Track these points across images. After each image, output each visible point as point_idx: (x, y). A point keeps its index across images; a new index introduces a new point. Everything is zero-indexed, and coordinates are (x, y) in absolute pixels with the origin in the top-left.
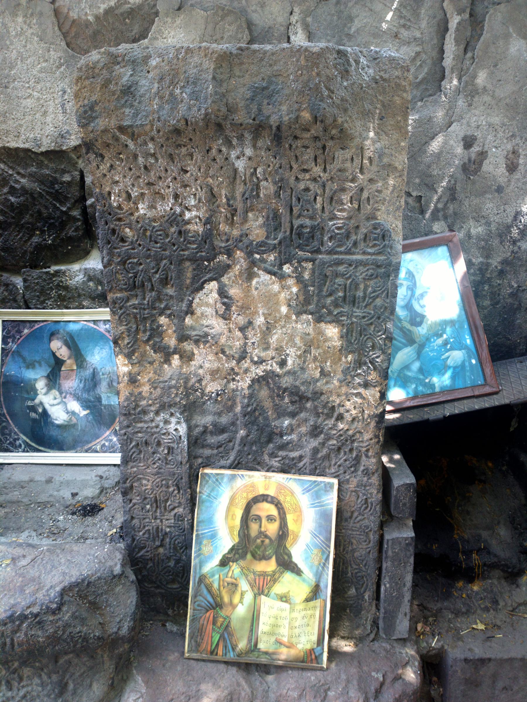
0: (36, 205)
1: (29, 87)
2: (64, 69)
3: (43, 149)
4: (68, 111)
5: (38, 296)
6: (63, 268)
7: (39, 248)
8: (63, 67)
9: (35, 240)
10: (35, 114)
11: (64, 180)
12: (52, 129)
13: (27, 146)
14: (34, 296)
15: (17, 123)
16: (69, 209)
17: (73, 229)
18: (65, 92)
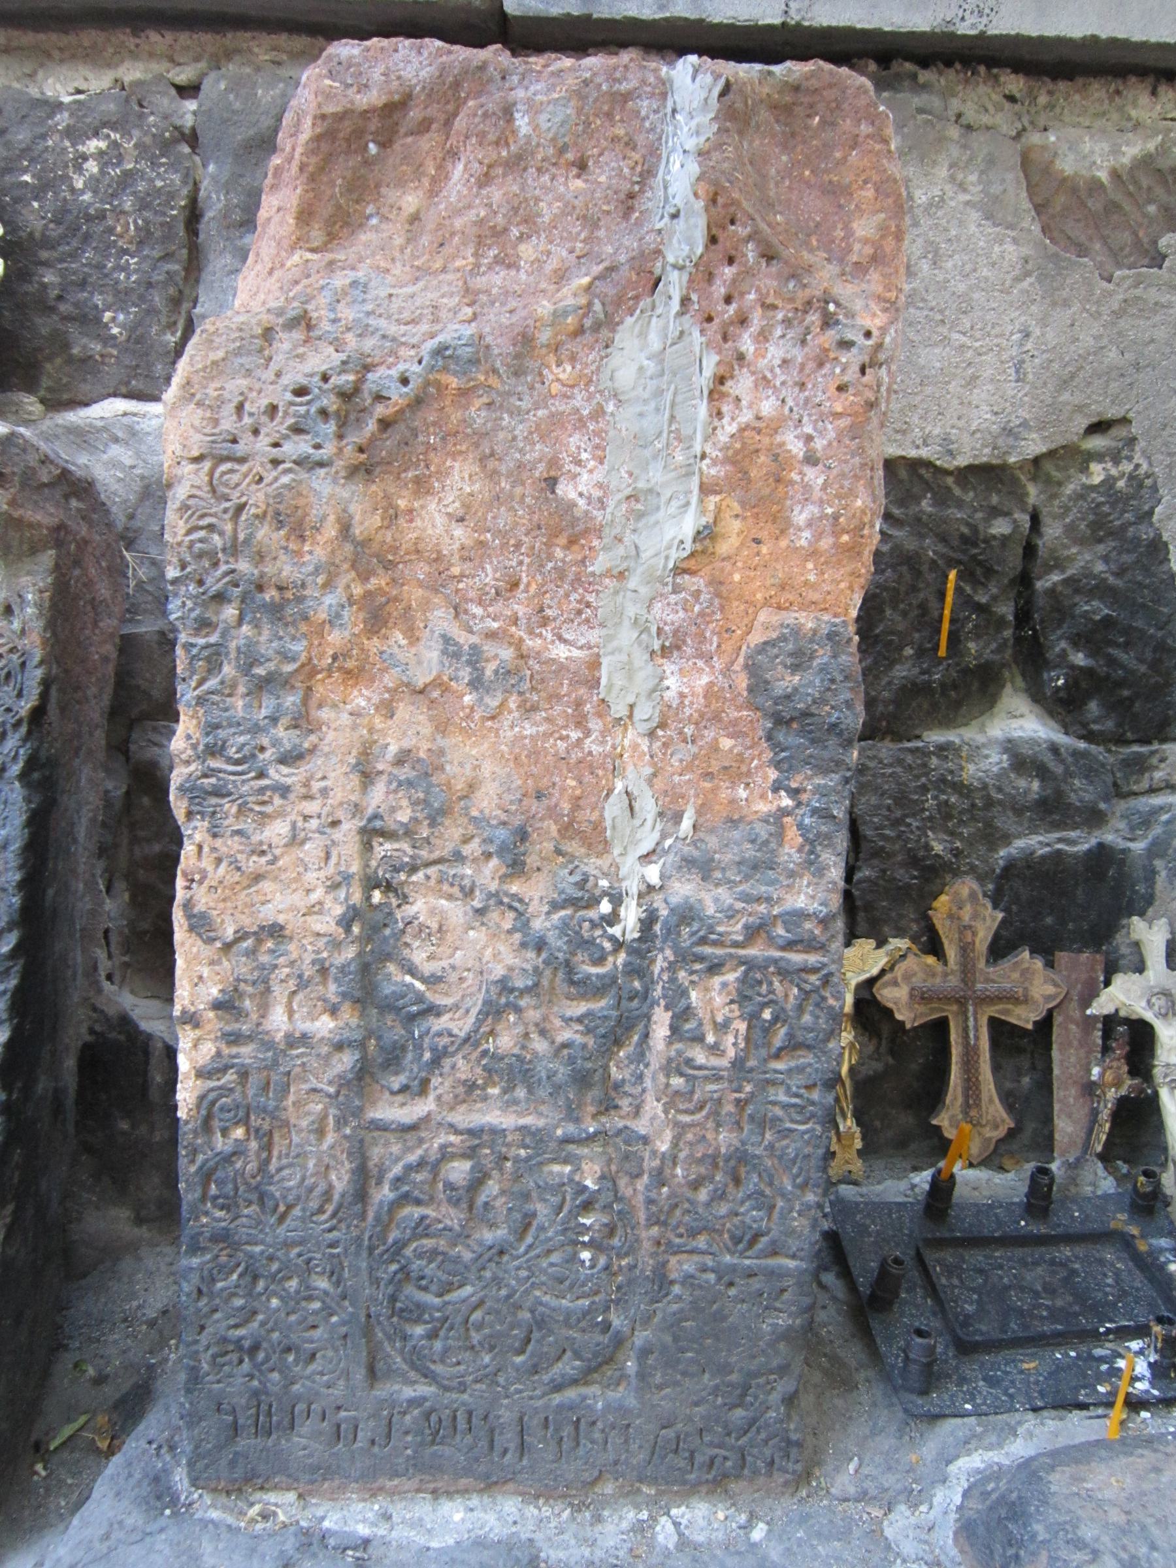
0: (919, 590)
1: (943, 321)
2: (1031, 284)
3: (962, 461)
4: (1030, 376)
5: (889, 808)
6: (951, 736)
7: (913, 691)
8: (1029, 280)
9: (901, 672)
10: (948, 383)
11: (994, 531)
12: (988, 416)
13: (924, 453)
15: (904, 402)
16: (995, 598)
17: (994, 646)
18: (1027, 335)
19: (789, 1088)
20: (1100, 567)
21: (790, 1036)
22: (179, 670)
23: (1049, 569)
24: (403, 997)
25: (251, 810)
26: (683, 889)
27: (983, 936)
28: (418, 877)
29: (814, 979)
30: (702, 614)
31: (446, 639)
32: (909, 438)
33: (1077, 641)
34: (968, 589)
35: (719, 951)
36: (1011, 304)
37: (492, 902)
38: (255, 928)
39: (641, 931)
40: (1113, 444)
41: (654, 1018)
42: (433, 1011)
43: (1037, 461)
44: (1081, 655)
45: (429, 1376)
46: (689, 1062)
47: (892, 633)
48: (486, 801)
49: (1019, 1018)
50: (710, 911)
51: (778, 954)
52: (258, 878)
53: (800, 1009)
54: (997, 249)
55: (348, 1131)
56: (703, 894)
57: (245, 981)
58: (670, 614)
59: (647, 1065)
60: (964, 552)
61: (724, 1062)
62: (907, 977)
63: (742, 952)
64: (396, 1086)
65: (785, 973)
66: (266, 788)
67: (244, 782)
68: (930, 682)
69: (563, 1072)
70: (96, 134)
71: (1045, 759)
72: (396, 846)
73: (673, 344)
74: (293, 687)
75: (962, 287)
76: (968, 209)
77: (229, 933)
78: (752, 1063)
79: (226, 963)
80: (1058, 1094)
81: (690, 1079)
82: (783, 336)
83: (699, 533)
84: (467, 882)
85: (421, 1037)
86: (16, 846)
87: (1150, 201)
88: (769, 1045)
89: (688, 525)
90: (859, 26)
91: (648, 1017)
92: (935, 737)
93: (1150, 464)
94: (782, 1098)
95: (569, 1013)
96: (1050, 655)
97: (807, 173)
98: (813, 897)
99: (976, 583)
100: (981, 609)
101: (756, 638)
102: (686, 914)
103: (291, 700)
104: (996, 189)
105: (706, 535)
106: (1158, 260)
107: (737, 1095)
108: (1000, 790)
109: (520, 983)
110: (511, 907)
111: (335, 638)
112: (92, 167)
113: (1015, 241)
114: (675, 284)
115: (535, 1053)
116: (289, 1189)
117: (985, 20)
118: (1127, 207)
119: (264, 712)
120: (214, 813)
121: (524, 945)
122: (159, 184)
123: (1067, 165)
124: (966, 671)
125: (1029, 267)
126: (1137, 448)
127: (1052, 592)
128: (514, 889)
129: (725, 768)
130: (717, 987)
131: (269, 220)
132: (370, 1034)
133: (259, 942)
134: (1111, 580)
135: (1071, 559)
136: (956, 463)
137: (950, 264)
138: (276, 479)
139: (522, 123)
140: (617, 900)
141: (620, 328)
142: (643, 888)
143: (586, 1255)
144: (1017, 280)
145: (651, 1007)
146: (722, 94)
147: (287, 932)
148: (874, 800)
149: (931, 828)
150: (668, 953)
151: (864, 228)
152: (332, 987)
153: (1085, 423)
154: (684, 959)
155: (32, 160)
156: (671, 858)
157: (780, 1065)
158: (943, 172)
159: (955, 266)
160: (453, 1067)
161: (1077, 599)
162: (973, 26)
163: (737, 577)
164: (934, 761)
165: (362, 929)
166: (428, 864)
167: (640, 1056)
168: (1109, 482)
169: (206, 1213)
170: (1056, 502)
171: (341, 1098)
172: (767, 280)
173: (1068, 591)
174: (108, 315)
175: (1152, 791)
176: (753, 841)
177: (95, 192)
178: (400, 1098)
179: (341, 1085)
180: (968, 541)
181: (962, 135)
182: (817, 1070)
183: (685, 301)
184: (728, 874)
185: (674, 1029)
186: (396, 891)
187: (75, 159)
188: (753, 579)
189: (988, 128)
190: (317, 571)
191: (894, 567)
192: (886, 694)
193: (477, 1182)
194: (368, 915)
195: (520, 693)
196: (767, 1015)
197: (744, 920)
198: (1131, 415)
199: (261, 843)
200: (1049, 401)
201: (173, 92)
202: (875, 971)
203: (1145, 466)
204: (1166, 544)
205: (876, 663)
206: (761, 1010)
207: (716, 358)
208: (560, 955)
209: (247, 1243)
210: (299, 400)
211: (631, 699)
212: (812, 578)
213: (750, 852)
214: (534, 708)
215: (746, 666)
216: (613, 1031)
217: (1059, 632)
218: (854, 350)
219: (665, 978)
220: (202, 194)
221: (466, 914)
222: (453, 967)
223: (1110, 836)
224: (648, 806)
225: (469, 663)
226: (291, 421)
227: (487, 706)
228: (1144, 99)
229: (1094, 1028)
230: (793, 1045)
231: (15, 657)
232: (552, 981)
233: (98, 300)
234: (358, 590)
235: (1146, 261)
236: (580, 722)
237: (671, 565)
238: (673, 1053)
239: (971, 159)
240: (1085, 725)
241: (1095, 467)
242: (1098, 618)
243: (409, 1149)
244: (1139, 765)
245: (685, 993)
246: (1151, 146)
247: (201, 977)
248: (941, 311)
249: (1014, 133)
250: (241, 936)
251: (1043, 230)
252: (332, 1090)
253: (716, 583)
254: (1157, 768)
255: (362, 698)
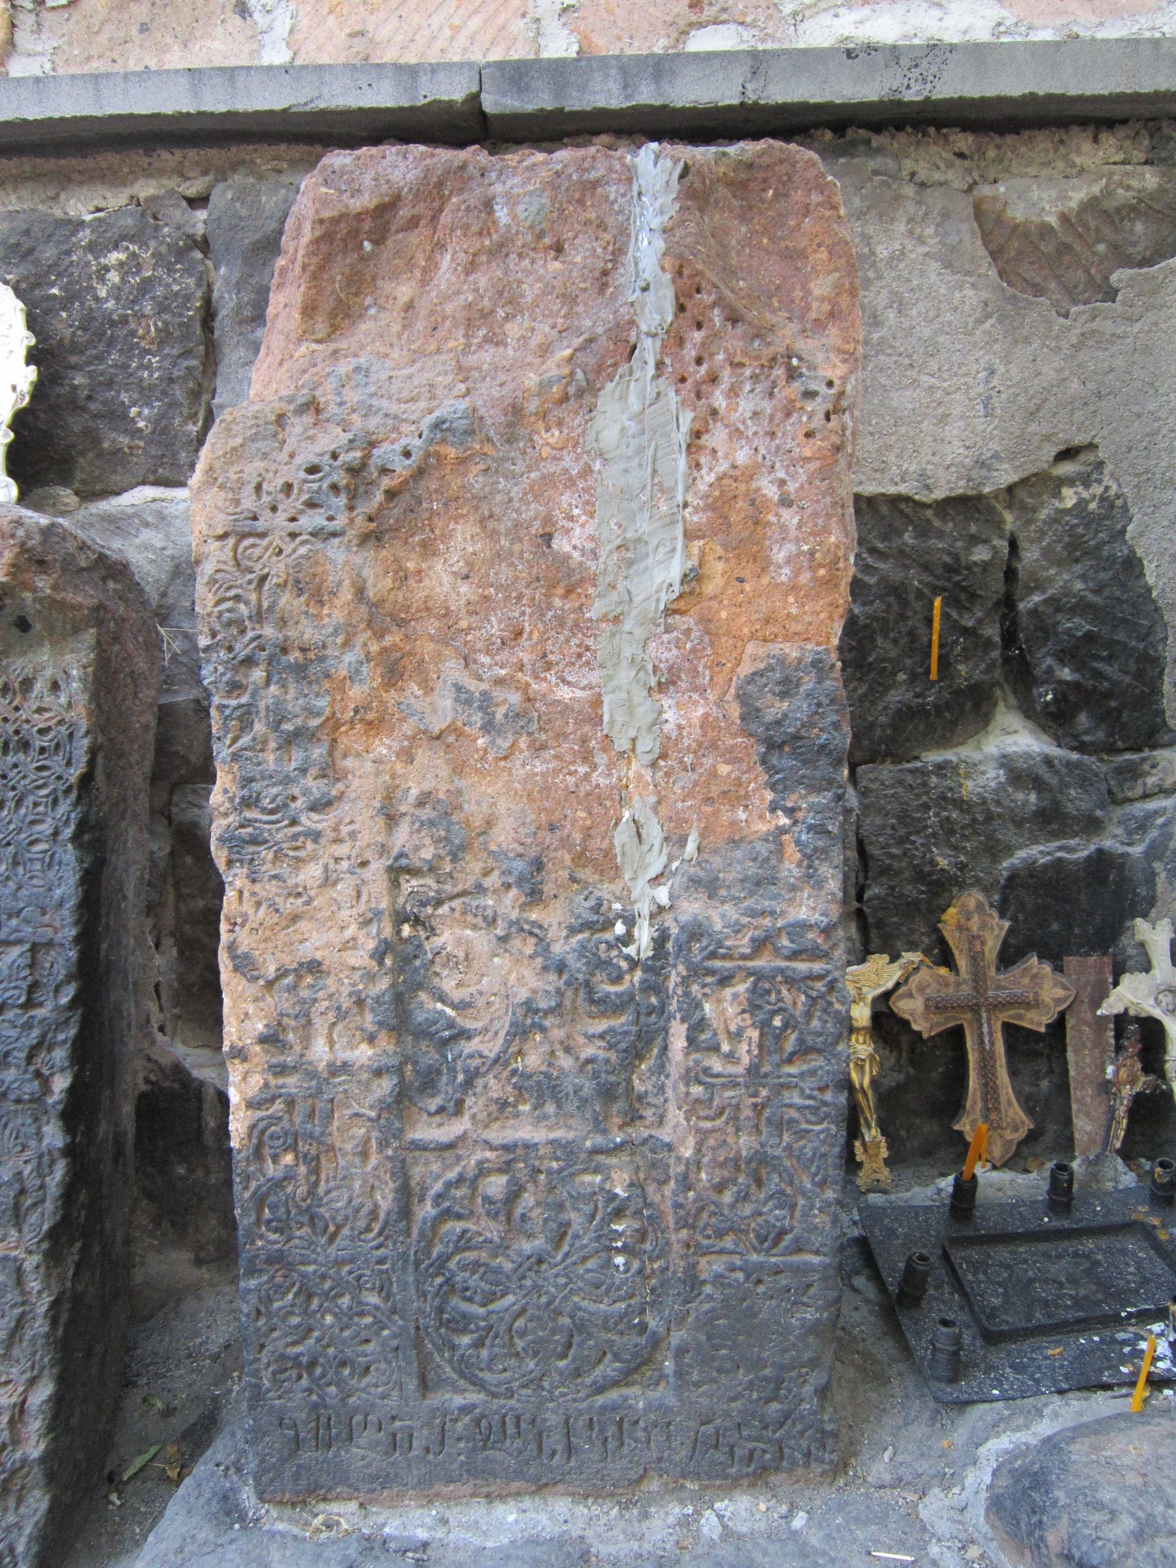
0: (907, 618)
1: (911, 365)
2: (992, 326)
3: (939, 494)
4: (998, 411)
5: (893, 828)
6: (950, 755)
7: (907, 714)
8: (990, 322)
9: (897, 697)
10: (920, 422)
13: (902, 489)
14: (883, 827)
16: (980, 621)
17: (983, 666)
18: (993, 373)
19: (802, 1090)
20: (1078, 586)
21: (801, 1041)
22: (214, 730)
23: (1030, 591)
24: (435, 1023)
25: (287, 855)
26: (692, 908)
27: (992, 946)
28: (444, 910)
29: (820, 986)
30: (693, 650)
31: (459, 688)
32: (887, 477)
33: (1062, 657)
34: (954, 615)
35: (728, 964)
36: (975, 345)
37: (513, 930)
38: (295, 965)
39: (655, 949)
40: (1083, 469)
41: (672, 1031)
42: (464, 1035)
43: (1010, 489)
44: (1067, 670)
45: (479, 1384)
46: (707, 1071)
47: (884, 660)
48: (503, 836)
49: (1031, 1021)
50: (718, 927)
51: (784, 964)
52: (295, 918)
53: (809, 1015)
54: (957, 295)
55: (390, 1152)
56: (710, 912)
57: (288, 1016)
58: (663, 653)
59: (667, 1076)
60: (949, 579)
61: (740, 1069)
62: (921, 989)
63: (750, 964)
64: (433, 1108)
65: (792, 981)
66: (299, 834)
67: (278, 830)
68: (923, 704)
69: (588, 1087)
70: (116, 247)
71: (1040, 772)
72: (422, 882)
73: (651, 405)
74: (319, 740)
75: (927, 333)
76: (928, 261)
77: (271, 971)
78: (766, 1069)
79: (269, 999)
80: (1075, 1094)
81: (709, 1087)
82: (752, 391)
83: (685, 575)
84: (489, 912)
85: (454, 1060)
86: (71, 903)
87: (1099, 241)
88: (782, 1050)
89: (675, 570)
90: (812, 101)
91: (666, 1030)
92: (933, 757)
93: (1119, 486)
94: (797, 1100)
95: (591, 1031)
96: (1038, 672)
97: (765, 241)
98: (814, 909)
99: (961, 608)
100: (965, 631)
101: (746, 669)
102: (695, 932)
103: (318, 752)
104: (953, 240)
105: (693, 578)
106: (1111, 294)
107: (754, 1100)
108: (998, 803)
109: (543, 1004)
110: (531, 933)
111: (356, 693)
112: (114, 277)
113: (974, 286)
114: (649, 350)
115: (561, 1069)
116: (337, 1210)
117: (929, 86)
118: (1078, 247)
119: (293, 765)
120: (252, 860)
121: (545, 969)
122: (176, 288)
123: (1018, 213)
124: (958, 693)
125: (989, 309)
126: (1106, 471)
127: (1034, 612)
128: (534, 916)
129: (724, 792)
130: (729, 998)
131: (277, 315)
132: (406, 1059)
133: (299, 977)
134: (1091, 597)
135: (1050, 580)
136: (933, 496)
137: (914, 312)
138: (294, 551)
139: (502, 214)
140: (630, 922)
141: (602, 393)
142: (654, 908)
143: (620, 1260)
144: (980, 322)
145: (668, 1020)
146: (682, 176)
147: (324, 968)
148: (879, 821)
149: (935, 844)
150: (681, 968)
151: (821, 287)
152: (369, 1017)
153: (1054, 450)
154: (696, 974)
155: (59, 275)
156: (678, 878)
157: (793, 1069)
158: (901, 227)
159: (919, 313)
160: (485, 1087)
161: (1059, 617)
162: (919, 92)
163: (724, 614)
164: (934, 780)
165: (394, 962)
166: (452, 898)
167: (661, 1068)
168: (1081, 504)
169: (261, 1237)
170: (1032, 527)
171: (382, 1121)
172: (734, 340)
173: (1050, 610)
174: (134, 411)
175: (1146, 796)
176: (754, 860)
177: (118, 299)
178: (437, 1119)
179: (381, 1109)
180: (952, 569)
181: (917, 193)
182: (828, 1072)
183: (660, 365)
184: (733, 891)
185: (691, 1040)
186: (423, 924)
187: (98, 271)
188: (738, 615)
189: (941, 184)
190: (336, 632)
191: (882, 598)
192: (883, 719)
193: (513, 1196)
194: (399, 948)
195: (529, 734)
196: (777, 1022)
197: (750, 934)
198: (1096, 440)
199: (297, 886)
200: (1018, 432)
201: (184, 204)
202: (890, 985)
203: (1114, 488)
204: (1140, 560)
205: (871, 689)
206: (771, 1019)
207: (690, 415)
208: (580, 976)
209: (301, 1263)
210: (311, 477)
211: (632, 733)
212: (794, 611)
213: (752, 869)
214: (544, 747)
215: (738, 696)
216: (633, 1045)
217: (1044, 650)
218: (819, 399)
219: (680, 992)
220: (215, 294)
221: (490, 941)
222: (481, 993)
223: (1110, 841)
224: (654, 832)
225: (480, 708)
226: (305, 497)
227: (499, 747)
228: (1087, 146)
229: (1106, 1029)
230: (804, 1050)
231: (63, 729)
232: (574, 1001)
233: (125, 397)
234: (374, 648)
235: (1100, 296)
236: (587, 757)
237: (662, 607)
238: (691, 1063)
239: (927, 214)
240: (1076, 737)
241: (1067, 492)
242: (1080, 634)
243: (446, 1168)
244: (1132, 773)
245: (698, 1006)
246: (1096, 189)
247: (247, 1014)
248: (909, 356)
249: (966, 187)
250: (282, 973)
251: (1000, 274)
252: (373, 1114)
253: (706, 621)
254: (1149, 774)
255: (383, 747)
